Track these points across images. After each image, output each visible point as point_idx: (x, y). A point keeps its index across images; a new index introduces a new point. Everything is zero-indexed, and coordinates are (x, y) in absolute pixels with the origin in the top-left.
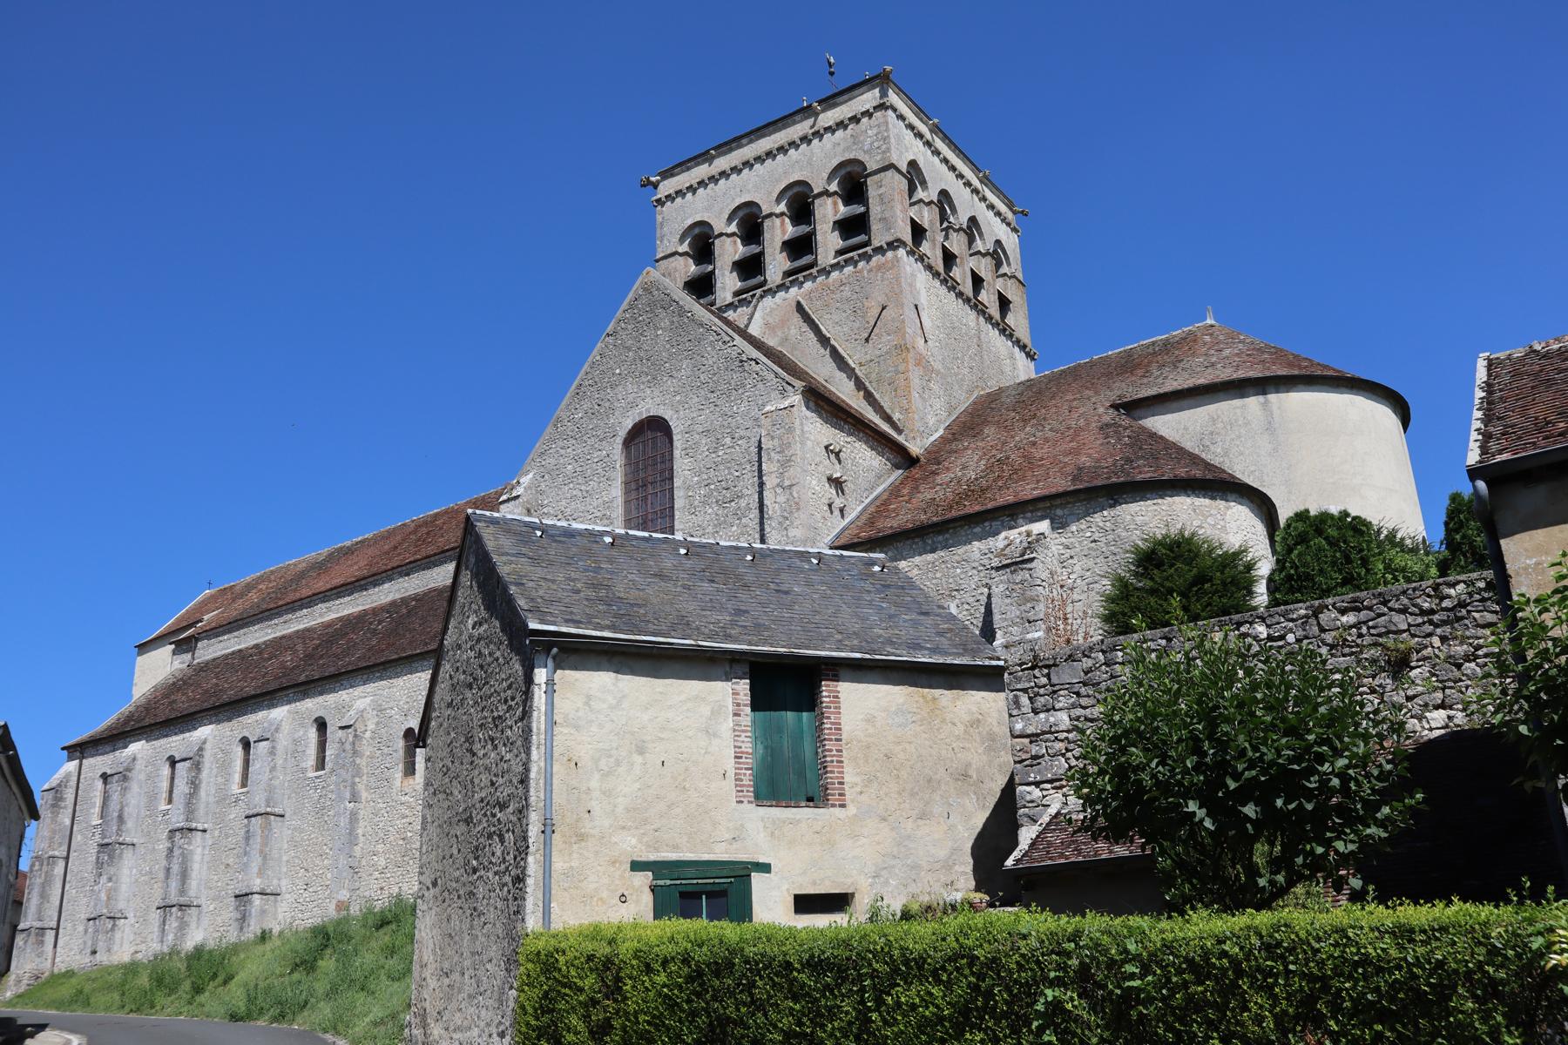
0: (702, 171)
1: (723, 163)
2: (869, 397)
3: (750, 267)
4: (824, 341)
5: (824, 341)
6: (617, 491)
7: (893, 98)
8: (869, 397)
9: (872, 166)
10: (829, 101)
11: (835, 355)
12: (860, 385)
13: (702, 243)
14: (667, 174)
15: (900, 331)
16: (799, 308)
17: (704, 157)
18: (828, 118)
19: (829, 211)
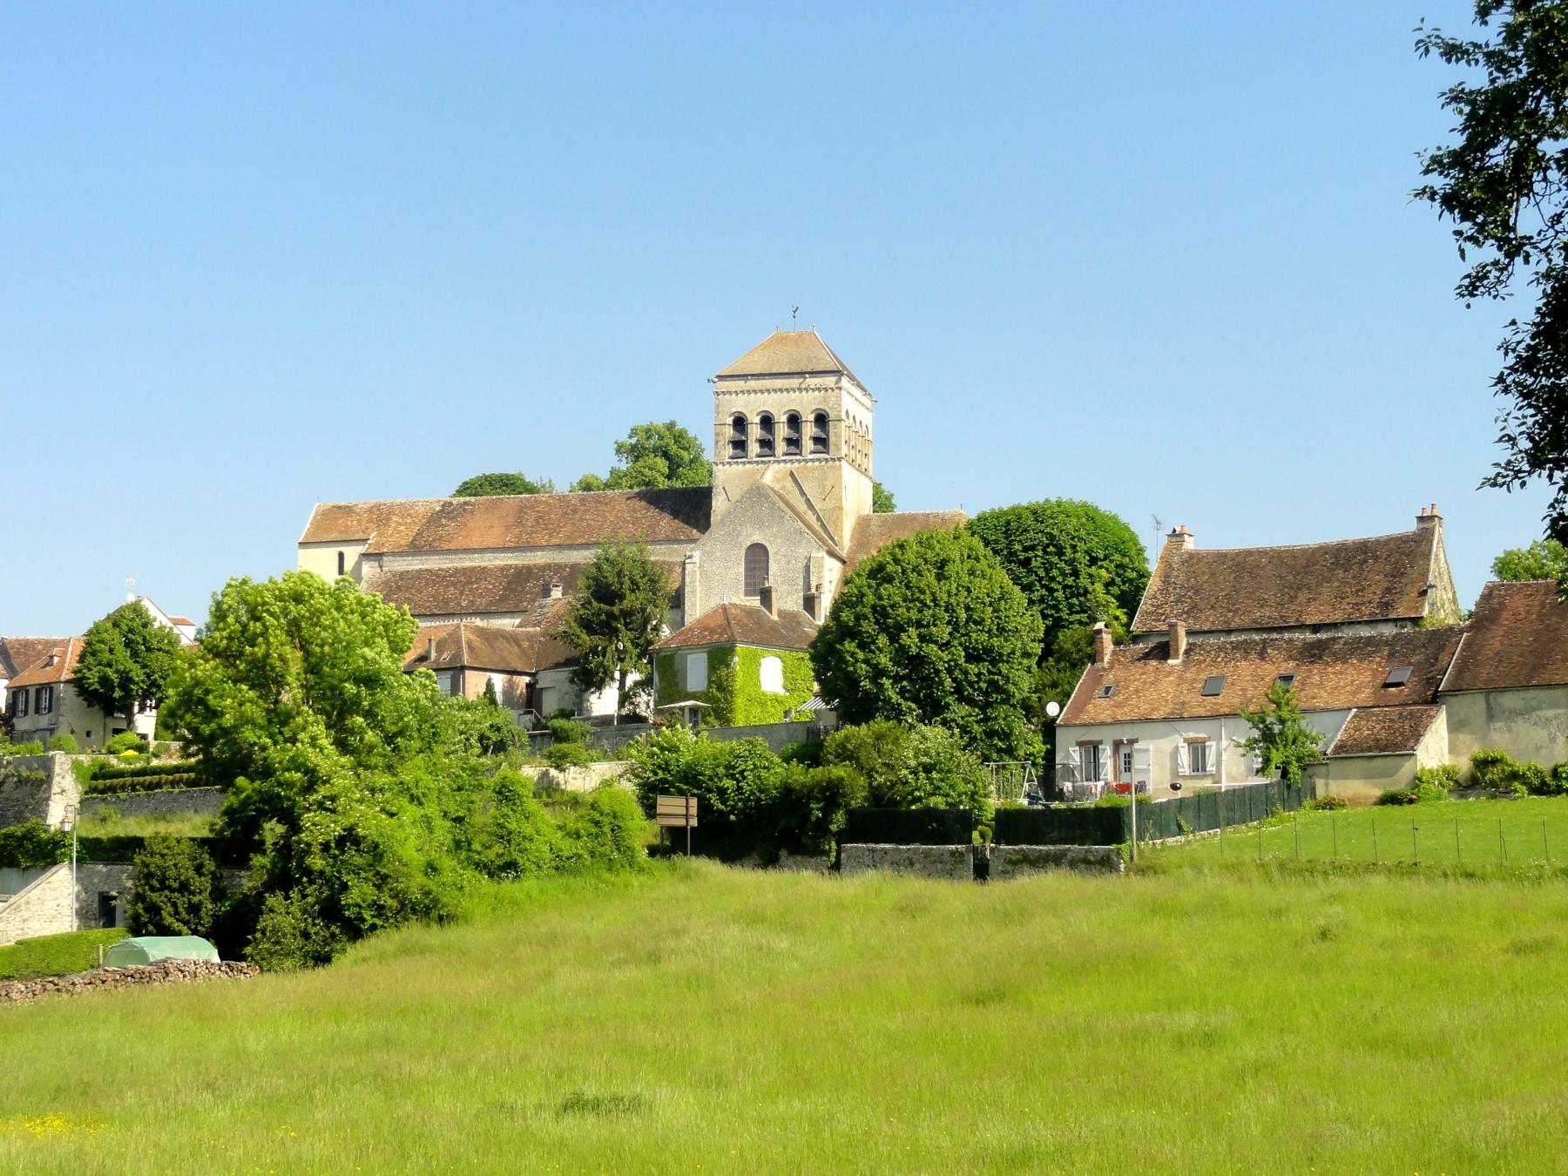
0: (741, 384)
1: (753, 384)
2: (823, 526)
3: (767, 444)
4: (803, 493)
5: (803, 493)
6: (742, 569)
7: (845, 382)
8: (823, 526)
9: (832, 415)
10: (813, 373)
11: (808, 502)
12: (819, 519)
13: (740, 423)
14: (721, 378)
15: (840, 500)
16: (792, 474)
17: (744, 377)
18: (812, 381)
19: (809, 430)
